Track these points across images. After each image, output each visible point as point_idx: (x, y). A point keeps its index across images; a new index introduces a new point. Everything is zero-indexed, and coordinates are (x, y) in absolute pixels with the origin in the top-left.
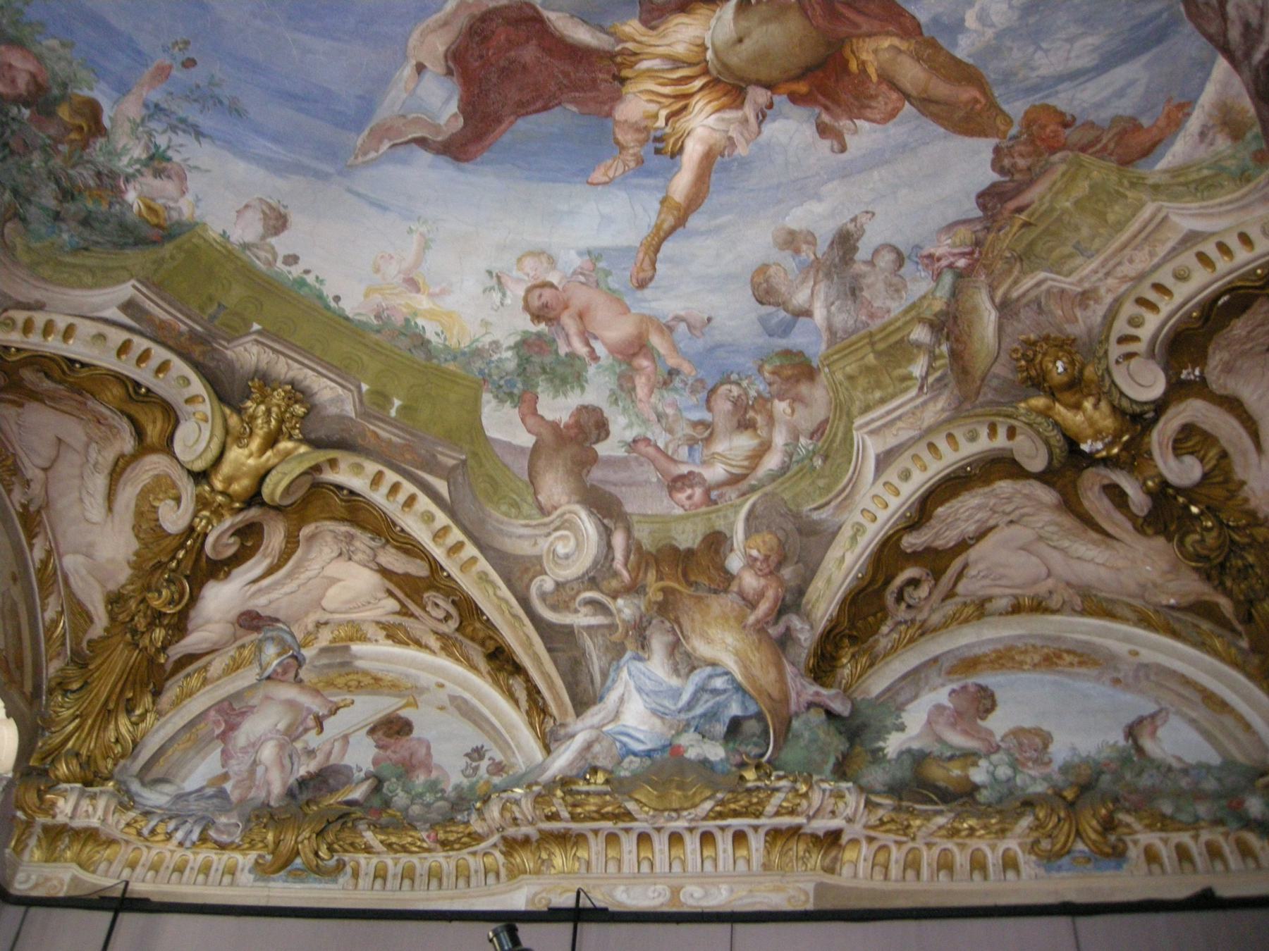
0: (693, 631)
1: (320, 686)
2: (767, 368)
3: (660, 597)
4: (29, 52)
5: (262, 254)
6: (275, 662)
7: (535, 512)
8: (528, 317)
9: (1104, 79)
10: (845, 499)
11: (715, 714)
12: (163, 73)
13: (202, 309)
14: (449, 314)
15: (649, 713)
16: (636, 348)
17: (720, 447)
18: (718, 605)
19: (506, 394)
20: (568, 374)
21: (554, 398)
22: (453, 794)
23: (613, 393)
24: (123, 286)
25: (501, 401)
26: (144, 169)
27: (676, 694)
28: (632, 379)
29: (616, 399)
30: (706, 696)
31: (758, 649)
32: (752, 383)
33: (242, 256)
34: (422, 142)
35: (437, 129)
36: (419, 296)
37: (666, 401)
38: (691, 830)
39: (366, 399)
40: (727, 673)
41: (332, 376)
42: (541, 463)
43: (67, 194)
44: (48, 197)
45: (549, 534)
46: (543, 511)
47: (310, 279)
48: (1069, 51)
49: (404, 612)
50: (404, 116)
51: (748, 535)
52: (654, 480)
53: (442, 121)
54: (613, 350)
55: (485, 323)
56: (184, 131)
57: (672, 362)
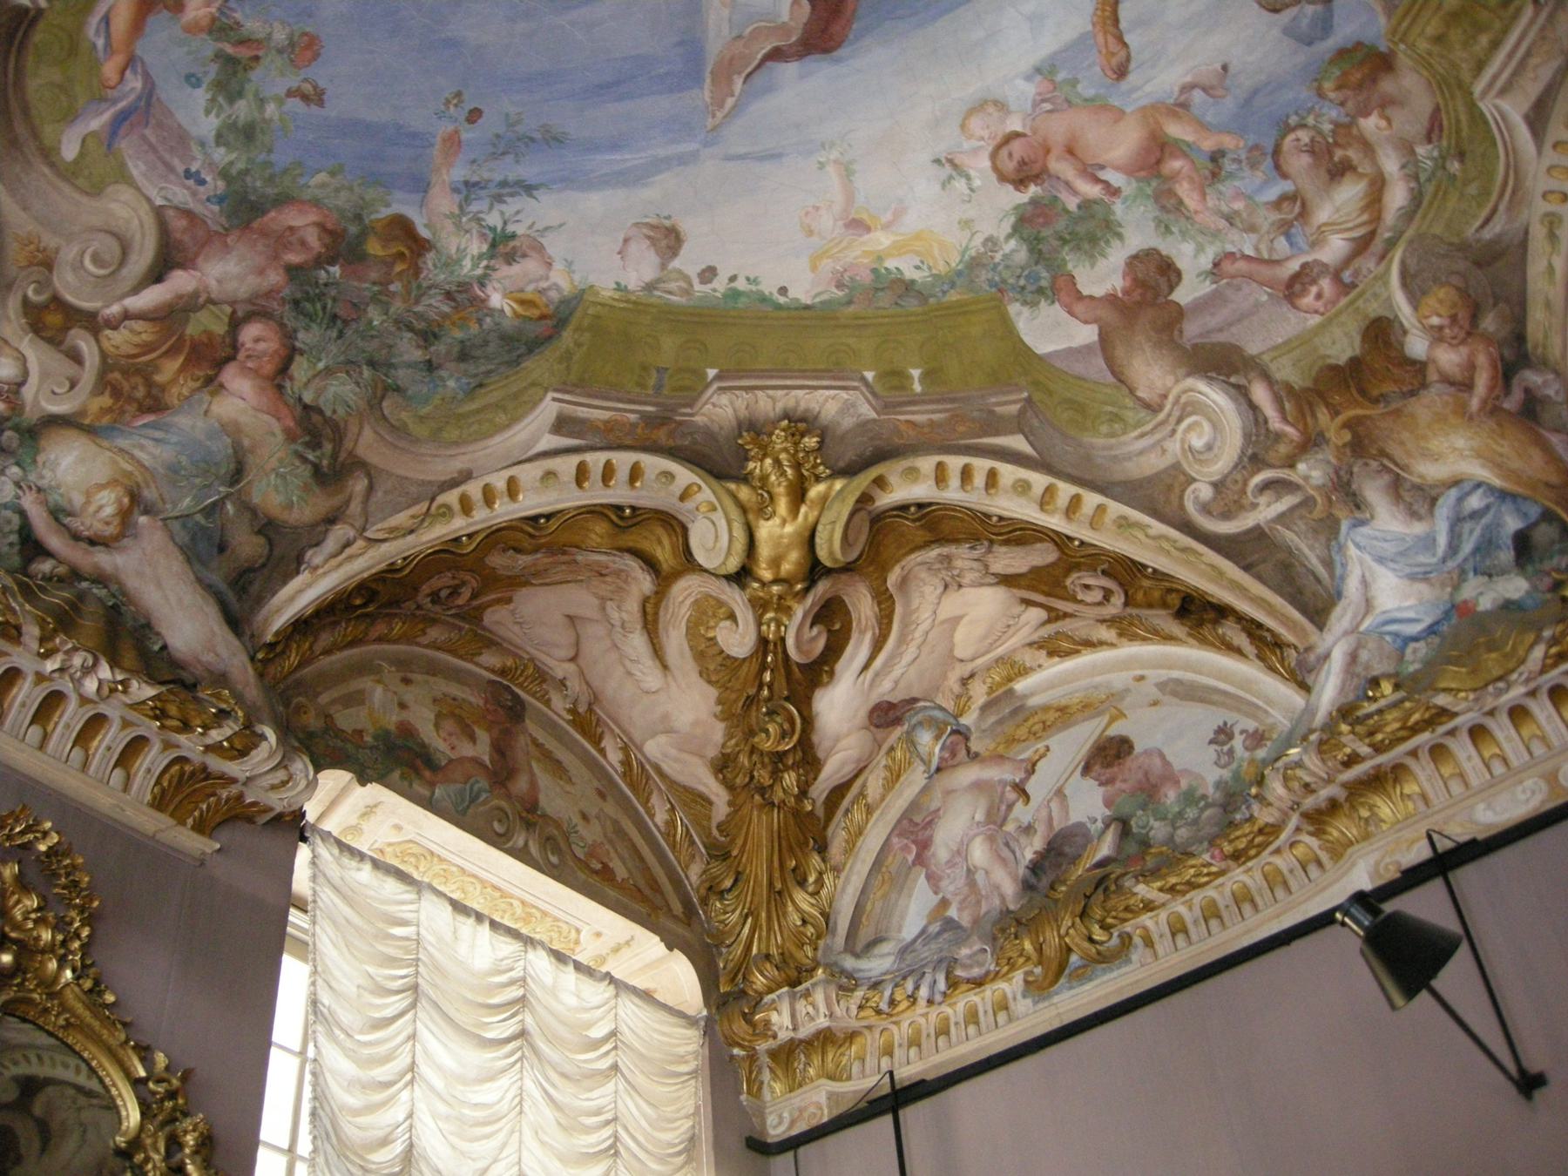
0: (1409, 454)
1: (1001, 749)
2: (1328, 85)
3: (1347, 436)
4: (303, 202)
5: (673, 286)
6: (937, 750)
7: (1143, 413)
8: (1011, 188)
10: (1514, 192)
11: (1490, 542)
12: (453, 143)
13: (642, 386)
14: (918, 237)
15: (1407, 582)
16: (1155, 155)
17: (1323, 214)
18: (1424, 407)
19: (1035, 294)
20: (1093, 228)
21: (1093, 266)
22: (1218, 795)
23: (1158, 222)
25: (1033, 304)
27: (1429, 542)
28: (1171, 193)
29: (1167, 227)
30: (1467, 526)
31: (1502, 436)
32: (1318, 116)
33: (652, 300)
34: (776, 55)
35: (783, 29)
36: (872, 235)
37: (1227, 197)
38: (1532, 694)
39: (878, 389)
40: (1479, 485)
41: (825, 383)
42: (1120, 352)
43: (428, 336)
44: (409, 350)
45: (1174, 431)
46: (1152, 408)
47: (741, 285)
49: (1055, 616)
50: (739, 37)
51: (1415, 302)
52: (1265, 298)
53: (785, 17)
54: (1129, 170)
55: (966, 224)
56: (512, 195)
57: (1208, 144)
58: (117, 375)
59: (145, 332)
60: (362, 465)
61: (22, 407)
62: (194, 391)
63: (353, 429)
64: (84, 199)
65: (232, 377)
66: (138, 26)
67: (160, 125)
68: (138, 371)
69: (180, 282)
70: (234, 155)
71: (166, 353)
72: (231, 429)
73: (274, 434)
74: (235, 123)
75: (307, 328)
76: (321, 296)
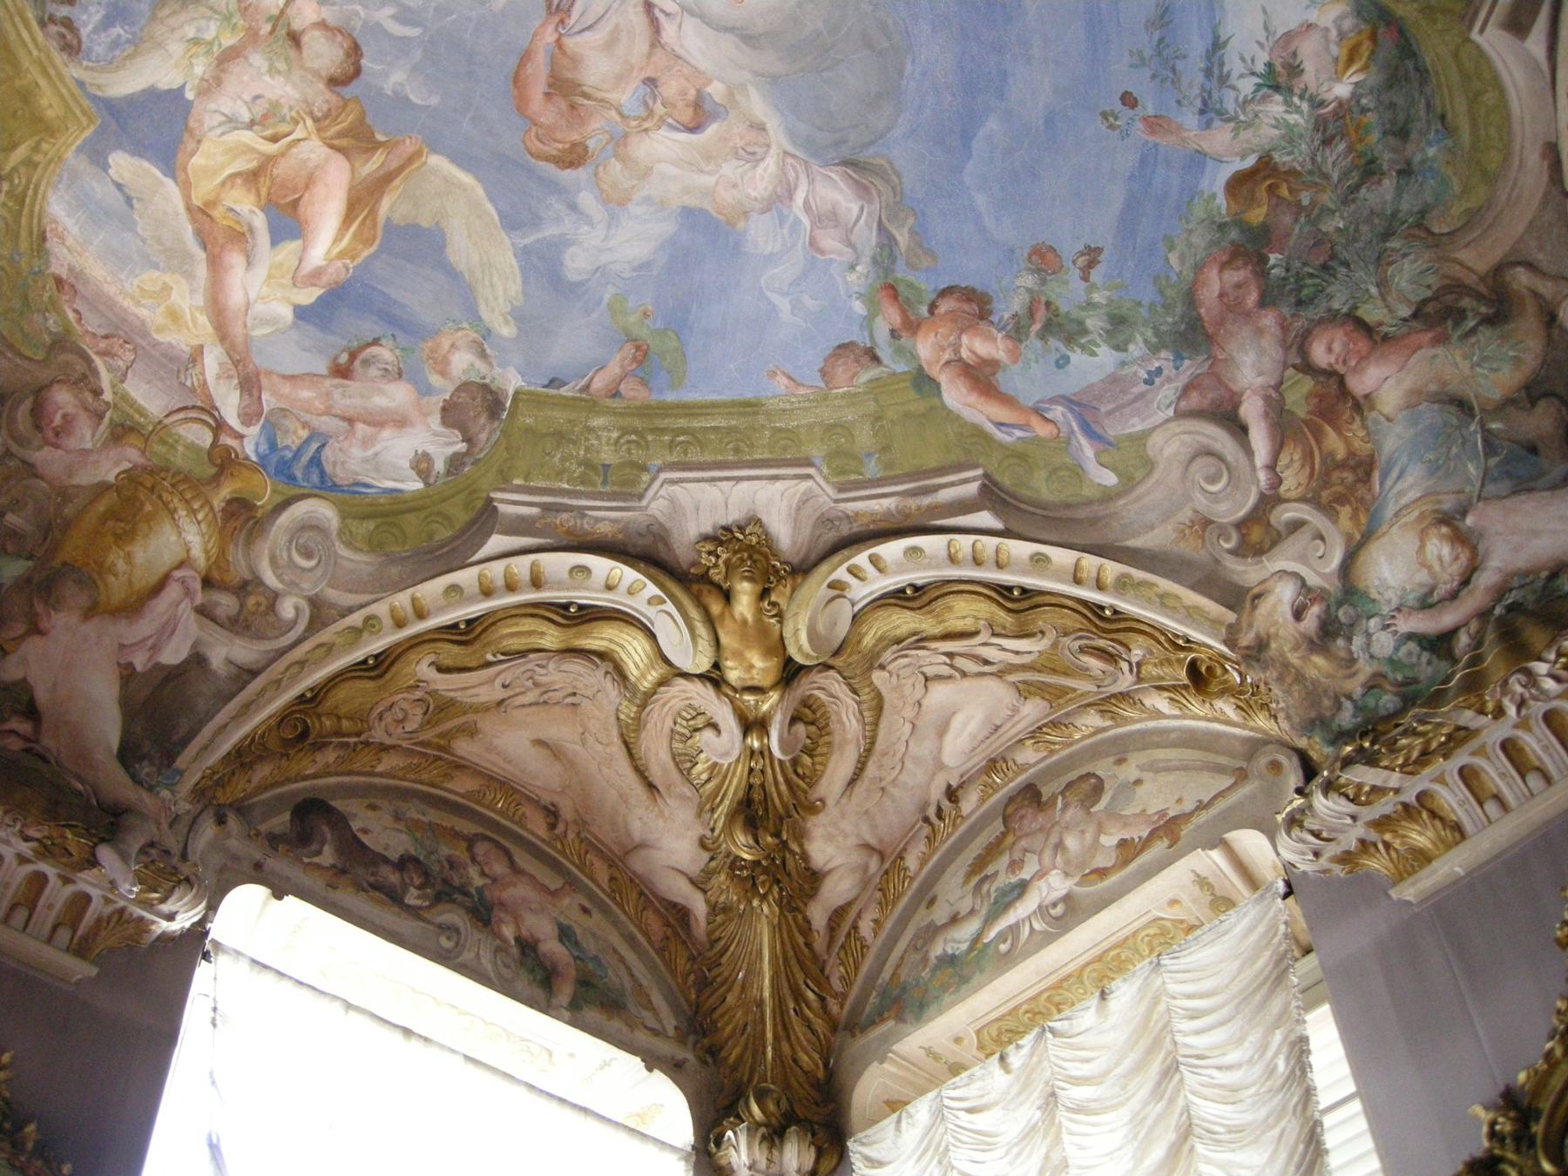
12: (1155, 124)
24: (1486, 46)
26: (1297, 91)
44: (1381, 194)
56: (1222, 64)
58: (1325, 494)
59: (1291, 457)
60: (1499, 269)
61: (1323, 590)
62: (1364, 427)
63: (1457, 271)
64: (1156, 476)
65: (1360, 384)
66: (1007, 400)
67: (1100, 398)
68: (1327, 473)
69: (1252, 411)
70: (1139, 338)
71: (1318, 442)
72: (1414, 400)
73: (1435, 357)
74: (1107, 332)
75: (1330, 297)
76: (1299, 277)
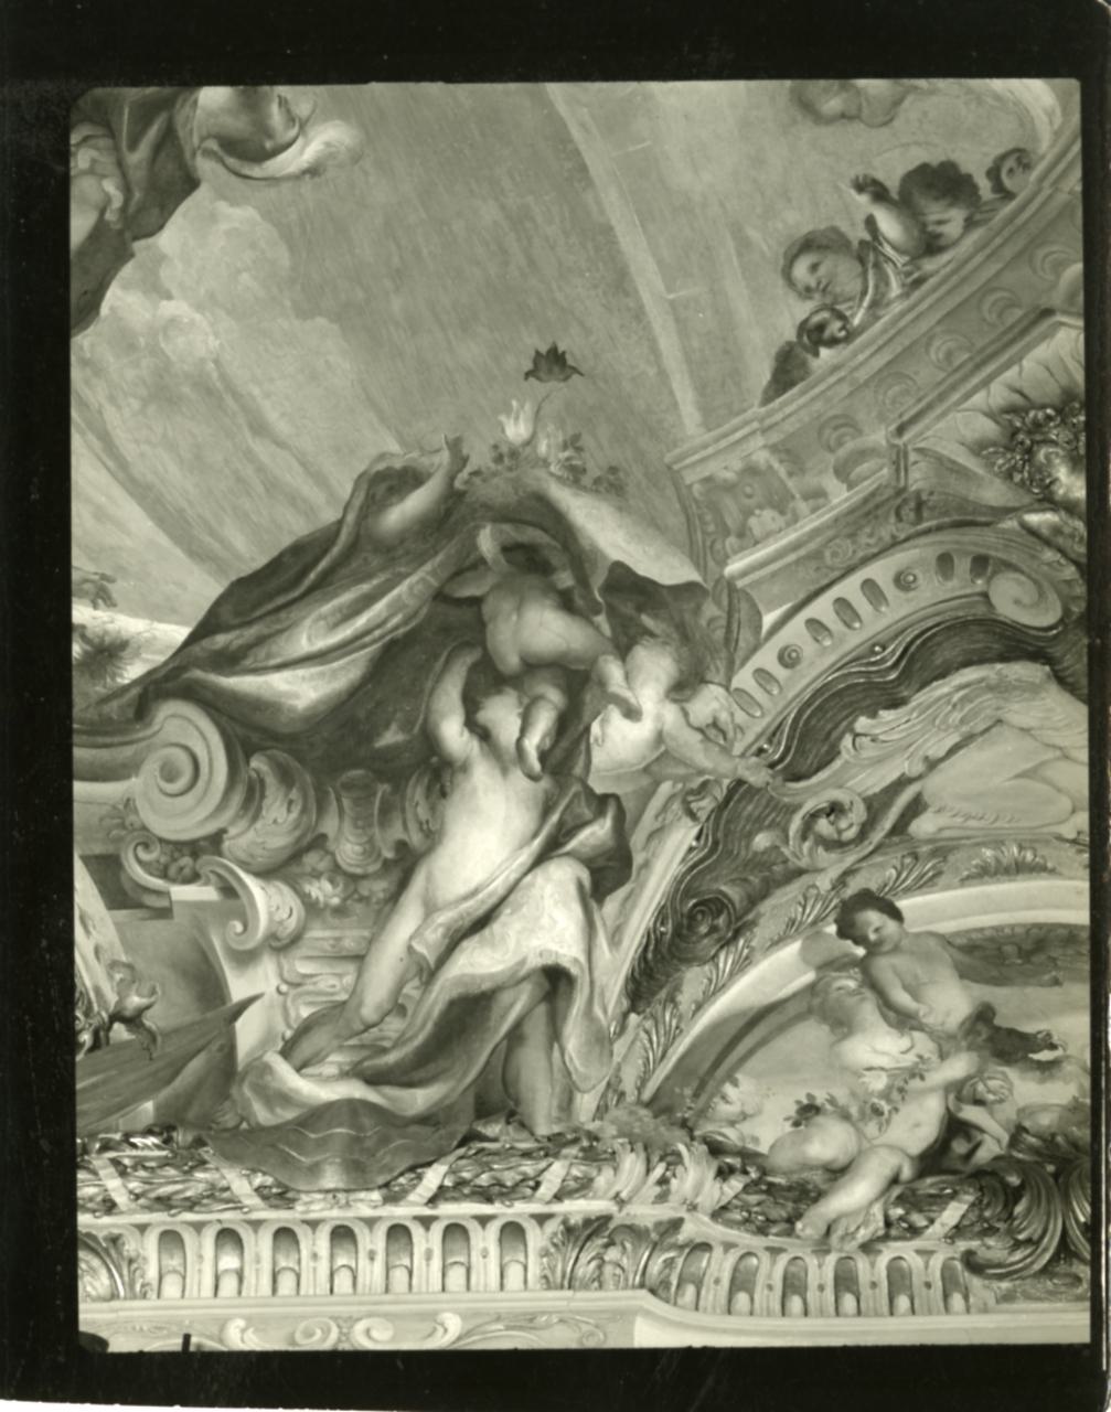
9: (118, 492)
48: (148, 442)
